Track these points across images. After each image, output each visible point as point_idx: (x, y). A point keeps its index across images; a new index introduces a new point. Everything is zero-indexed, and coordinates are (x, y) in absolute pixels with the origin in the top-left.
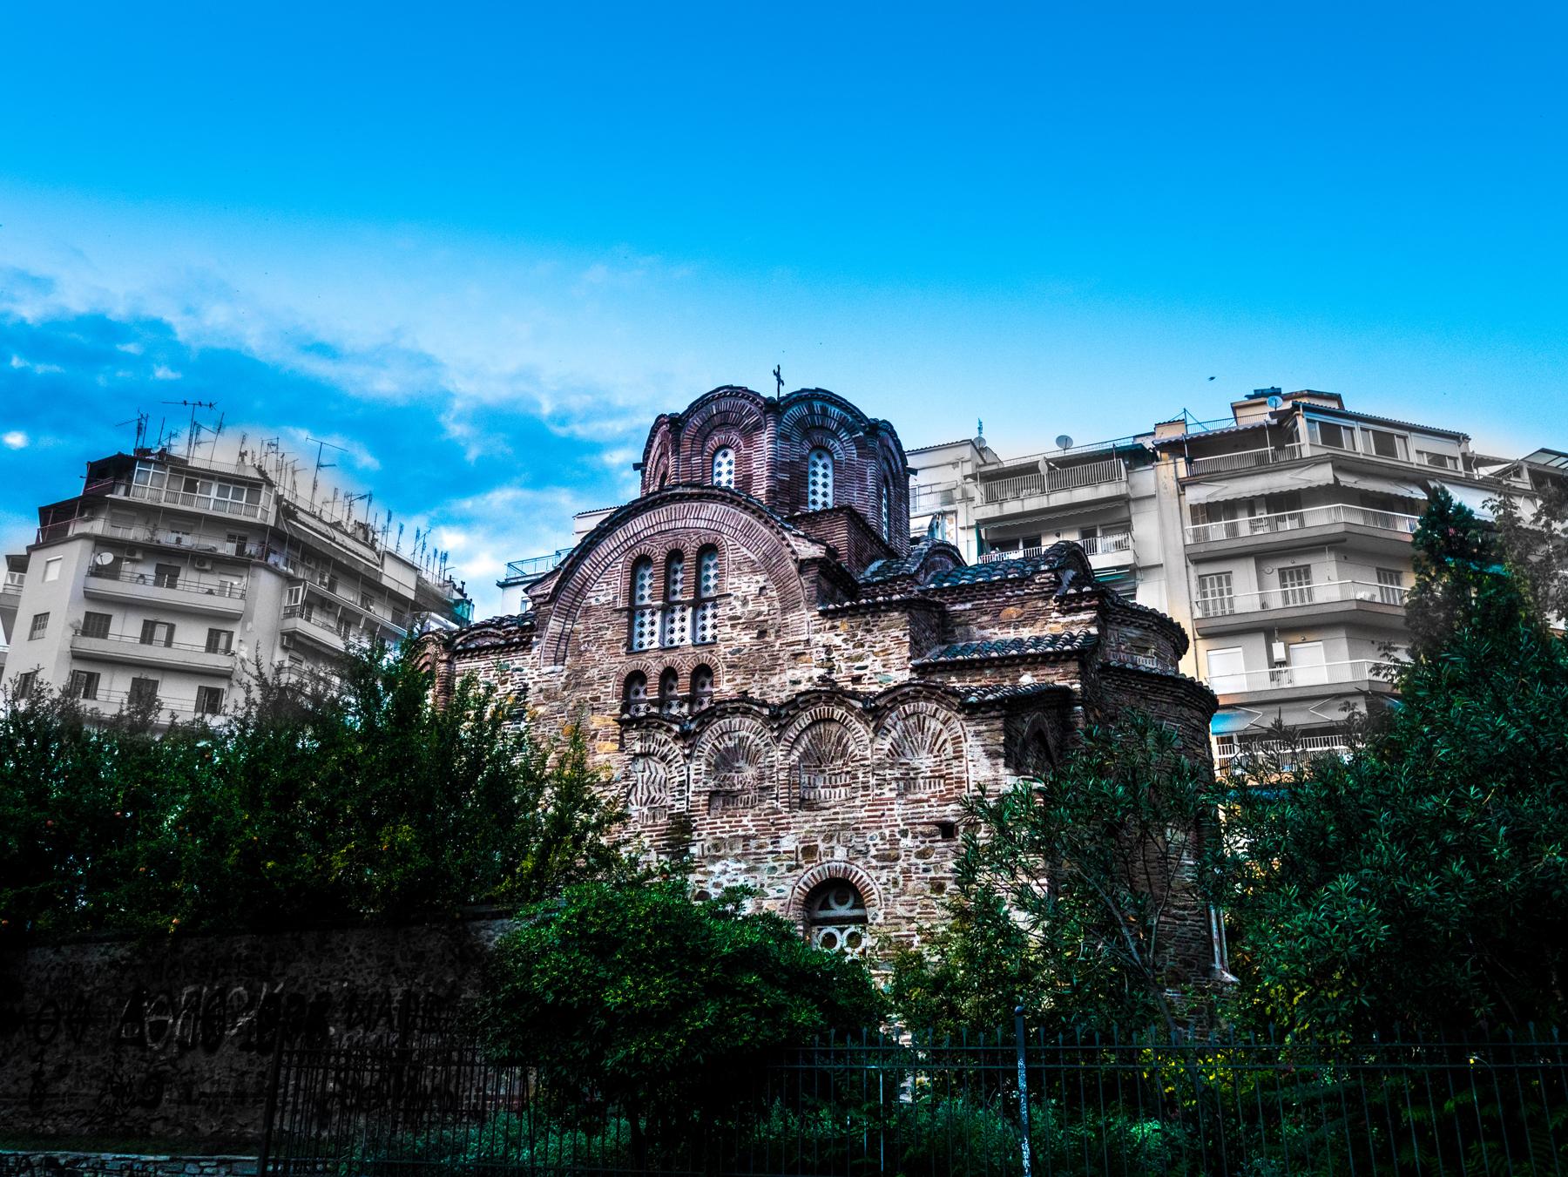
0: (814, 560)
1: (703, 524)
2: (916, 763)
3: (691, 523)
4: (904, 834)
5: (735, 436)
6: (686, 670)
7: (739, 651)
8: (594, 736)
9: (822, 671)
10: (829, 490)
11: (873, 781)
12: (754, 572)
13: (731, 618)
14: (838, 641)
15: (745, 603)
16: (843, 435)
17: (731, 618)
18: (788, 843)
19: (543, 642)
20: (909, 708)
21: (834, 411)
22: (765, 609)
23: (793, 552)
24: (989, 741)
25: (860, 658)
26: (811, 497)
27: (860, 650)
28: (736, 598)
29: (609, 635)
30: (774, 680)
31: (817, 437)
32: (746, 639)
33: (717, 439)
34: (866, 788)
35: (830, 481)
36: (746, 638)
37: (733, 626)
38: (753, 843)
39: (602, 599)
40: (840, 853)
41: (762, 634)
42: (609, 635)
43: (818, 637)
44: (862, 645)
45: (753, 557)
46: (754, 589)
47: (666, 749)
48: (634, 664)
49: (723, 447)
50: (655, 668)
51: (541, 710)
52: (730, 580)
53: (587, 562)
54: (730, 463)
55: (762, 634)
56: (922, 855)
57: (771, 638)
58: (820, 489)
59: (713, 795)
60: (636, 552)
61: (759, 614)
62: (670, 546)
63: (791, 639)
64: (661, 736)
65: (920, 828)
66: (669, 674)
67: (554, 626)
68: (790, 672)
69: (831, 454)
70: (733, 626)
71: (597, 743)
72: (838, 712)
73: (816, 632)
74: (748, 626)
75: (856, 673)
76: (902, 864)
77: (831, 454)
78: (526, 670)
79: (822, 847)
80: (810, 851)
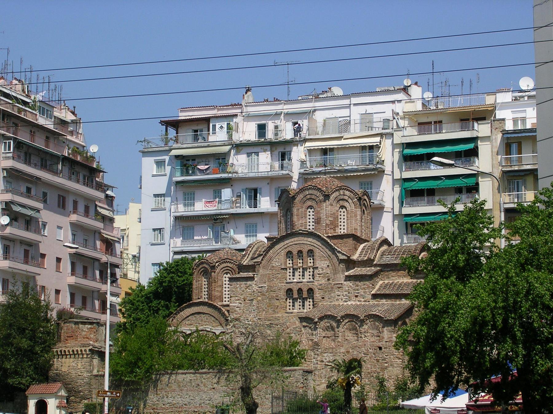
0: (344, 259)
1: (309, 243)
5: (313, 203)
6: (305, 290)
7: (321, 285)
10: (345, 221)
11: (363, 336)
12: (325, 260)
14: (351, 284)
15: (323, 269)
16: (350, 201)
18: (343, 350)
19: (259, 276)
21: (347, 193)
22: (329, 272)
25: (358, 290)
26: (340, 224)
30: (332, 295)
33: (309, 203)
34: (361, 337)
35: (345, 217)
36: (323, 281)
37: (319, 277)
38: (334, 350)
39: (277, 264)
40: (355, 353)
41: (329, 280)
46: (325, 266)
48: (289, 286)
49: (311, 207)
50: (295, 289)
53: (271, 251)
55: (329, 280)
56: (374, 354)
58: (342, 220)
59: (324, 337)
60: (287, 250)
62: (299, 249)
66: (300, 291)
67: (261, 271)
69: (346, 208)
70: (319, 277)
71: (278, 310)
74: (323, 277)
75: (356, 294)
77: (346, 208)
78: (253, 285)
79: (351, 351)
80: (348, 352)
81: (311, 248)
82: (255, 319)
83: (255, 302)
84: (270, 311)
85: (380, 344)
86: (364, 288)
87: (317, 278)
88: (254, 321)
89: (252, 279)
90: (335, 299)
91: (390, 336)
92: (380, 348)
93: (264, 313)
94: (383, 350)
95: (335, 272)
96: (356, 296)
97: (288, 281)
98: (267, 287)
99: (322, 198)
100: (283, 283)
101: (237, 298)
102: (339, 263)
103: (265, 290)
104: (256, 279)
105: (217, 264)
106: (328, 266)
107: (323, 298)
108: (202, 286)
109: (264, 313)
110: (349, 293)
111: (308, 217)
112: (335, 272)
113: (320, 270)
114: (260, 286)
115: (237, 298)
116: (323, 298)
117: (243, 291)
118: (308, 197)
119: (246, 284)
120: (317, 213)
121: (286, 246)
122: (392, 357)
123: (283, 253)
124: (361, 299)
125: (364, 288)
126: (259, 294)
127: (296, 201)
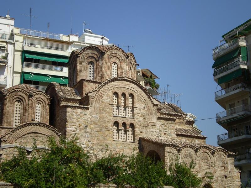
1: (131, 88)
2: (219, 163)
3: (128, 87)
4: (219, 177)
5: (117, 61)
7: (140, 122)
8: (107, 136)
9: (158, 131)
11: (213, 166)
12: (142, 103)
13: (137, 113)
15: (140, 111)
17: (137, 113)
20: (219, 152)
23: (152, 102)
24: (232, 162)
25: (166, 129)
27: (166, 127)
28: (138, 109)
29: (108, 110)
30: (148, 130)
31: (130, 64)
32: (141, 119)
33: (113, 60)
36: (141, 119)
42: (108, 110)
43: (157, 122)
44: (166, 127)
45: (142, 100)
46: (142, 107)
47: (174, 152)
51: (92, 126)
52: (137, 104)
54: (116, 67)
56: (222, 181)
57: (147, 120)
61: (144, 114)
63: (152, 122)
64: (173, 149)
65: (221, 176)
68: (151, 129)
72: (207, 151)
73: (157, 121)
74: (141, 116)
75: (165, 133)
76: (219, 182)
78: (88, 115)
81: (132, 92)
82: (89, 143)
83: (88, 129)
84: (101, 138)
85: (226, 174)
86: (171, 129)
87: (136, 116)
88: (88, 145)
89: (88, 109)
90: (150, 134)
91: (232, 168)
92: (226, 177)
93: (96, 139)
94: (228, 178)
95: (150, 114)
96: (165, 134)
97: (115, 115)
98: (99, 118)
99: (124, 58)
100: (111, 116)
101: (73, 124)
102: (153, 106)
103: (97, 120)
104: (90, 110)
105: (34, 94)
106: (144, 108)
107: (141, 132)
108: (13, 111)
109: (96, 139)
110: (160, 131)
111: (112, 70)
112: (150, 114)
113: (139, 110)
114: (93, 116)
115: (73, 124)
116: (141, 132)
117: (79, 118)
118: (114, 55)
119: (81, 113)
120: (119, 68)
121: (113, 88)
122: (234, 184)
123: (111, 92)
124: (169, 137)
125: (171, 129)
126: (92, 122)
127: (106, 55)
